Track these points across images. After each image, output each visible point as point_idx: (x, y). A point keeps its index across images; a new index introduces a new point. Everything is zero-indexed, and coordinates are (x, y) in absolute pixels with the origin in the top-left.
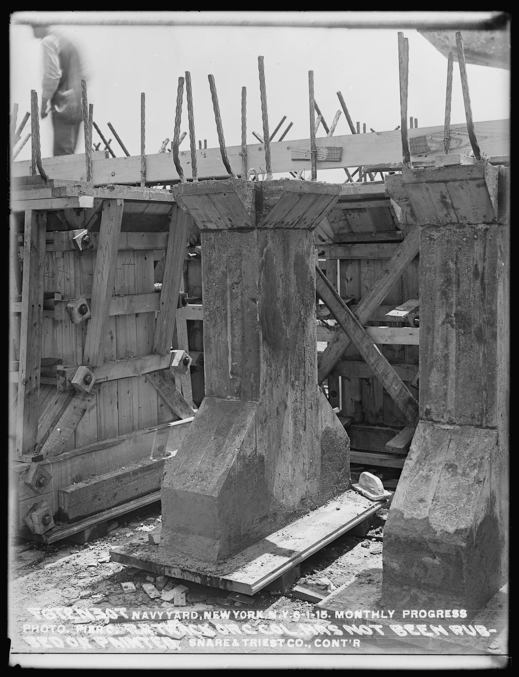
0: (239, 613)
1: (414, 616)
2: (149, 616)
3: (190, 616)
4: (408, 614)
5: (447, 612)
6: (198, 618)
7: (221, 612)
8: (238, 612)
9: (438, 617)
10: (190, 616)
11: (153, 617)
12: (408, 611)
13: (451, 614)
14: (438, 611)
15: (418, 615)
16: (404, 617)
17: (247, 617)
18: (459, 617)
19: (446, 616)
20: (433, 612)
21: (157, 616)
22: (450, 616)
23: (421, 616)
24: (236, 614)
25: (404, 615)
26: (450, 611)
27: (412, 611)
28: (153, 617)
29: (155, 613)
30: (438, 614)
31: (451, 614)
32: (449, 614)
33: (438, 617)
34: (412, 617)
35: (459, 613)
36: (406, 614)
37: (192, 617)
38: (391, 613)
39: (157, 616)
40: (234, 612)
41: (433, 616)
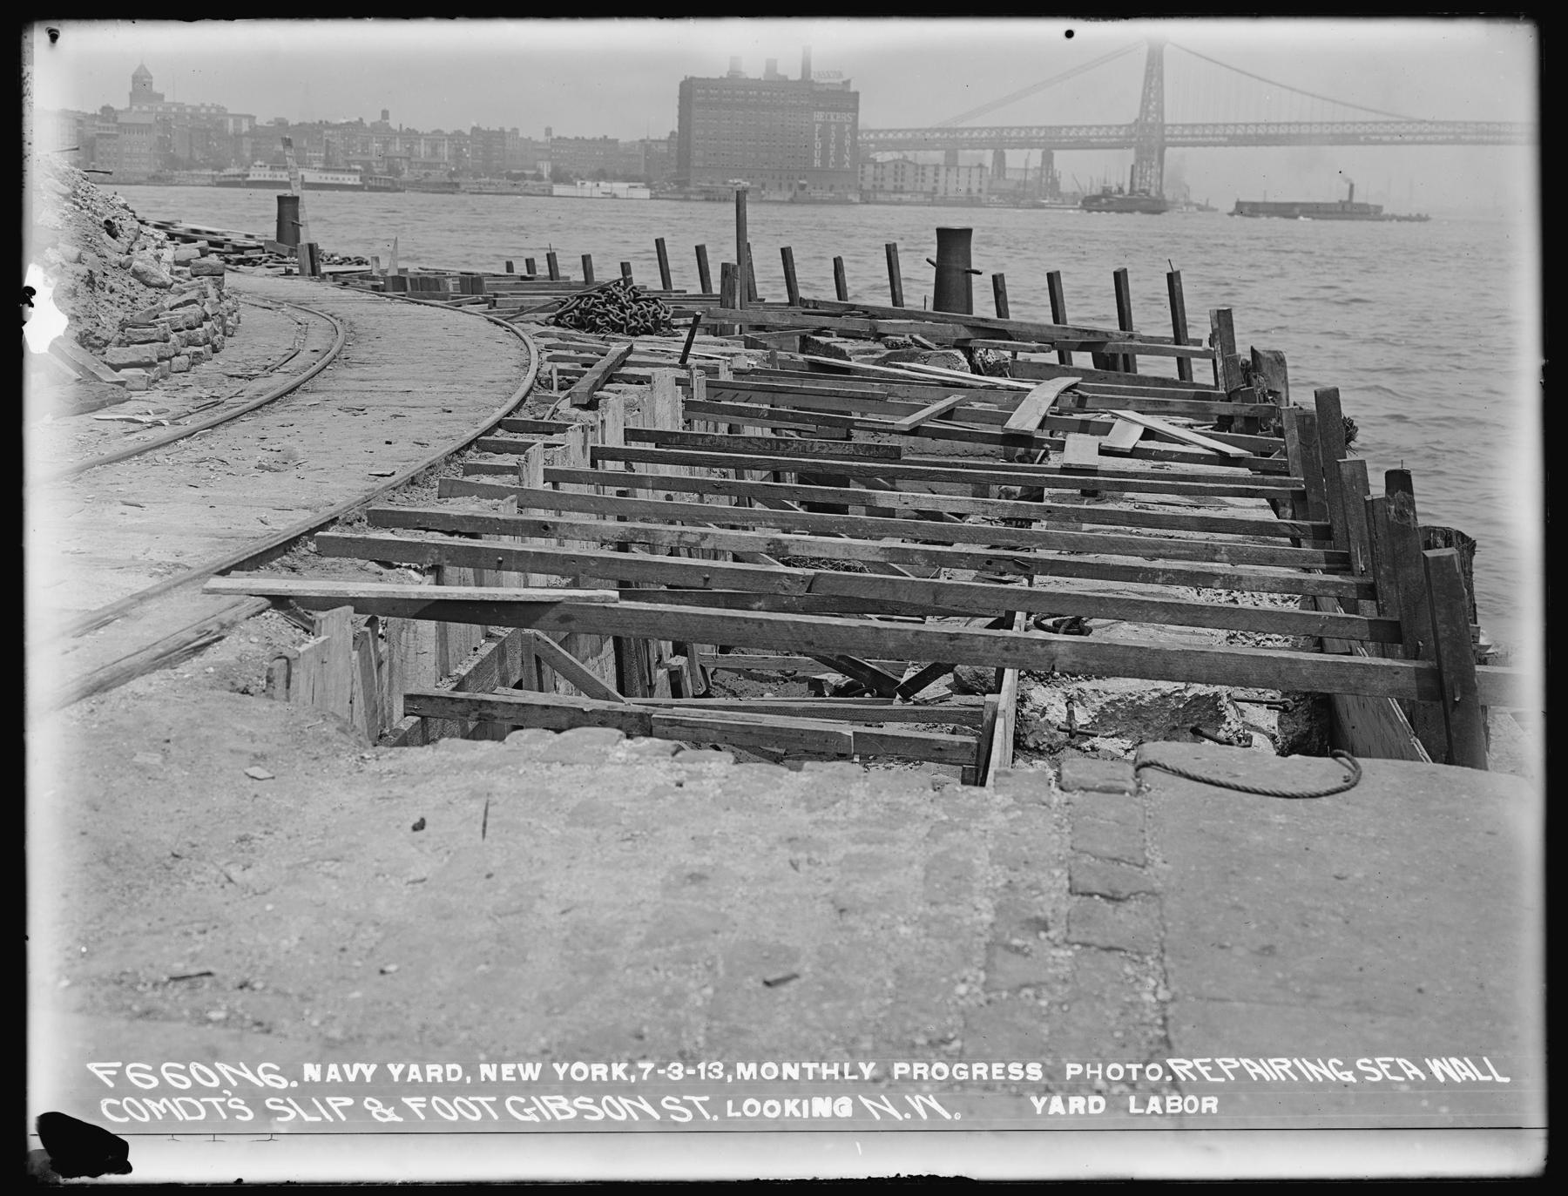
4: (906, 1071)
5: (997, 1068)
6: (463, 1079)
7: (520, 1066)
8: (566, 1065)
9: (975, 1077)
10: (444, 1076)
11: (352, 1078)
12: (907, 1066)
13: (1006, 1072)
14: (975, 1066)
16: (896, 1077)
18: (1024, 1080)
20: (964, 1066)
22: (1003, 1078)
24: (560, 1070)
25: (896, 1073)
26: (1002, 1065)
27: (916, 1065)
28: (352, 1078)
29: (357, 1066)
30: (975, 1073)
31: (1006, 1072)
32: (1001, 1072)
33: (975, 1077)
35: (1024, 1068)
36: (902, 1072)
37: (450, 1079)
38: (868, 1070)
40: (556, 1066)
41: (965, 1075)
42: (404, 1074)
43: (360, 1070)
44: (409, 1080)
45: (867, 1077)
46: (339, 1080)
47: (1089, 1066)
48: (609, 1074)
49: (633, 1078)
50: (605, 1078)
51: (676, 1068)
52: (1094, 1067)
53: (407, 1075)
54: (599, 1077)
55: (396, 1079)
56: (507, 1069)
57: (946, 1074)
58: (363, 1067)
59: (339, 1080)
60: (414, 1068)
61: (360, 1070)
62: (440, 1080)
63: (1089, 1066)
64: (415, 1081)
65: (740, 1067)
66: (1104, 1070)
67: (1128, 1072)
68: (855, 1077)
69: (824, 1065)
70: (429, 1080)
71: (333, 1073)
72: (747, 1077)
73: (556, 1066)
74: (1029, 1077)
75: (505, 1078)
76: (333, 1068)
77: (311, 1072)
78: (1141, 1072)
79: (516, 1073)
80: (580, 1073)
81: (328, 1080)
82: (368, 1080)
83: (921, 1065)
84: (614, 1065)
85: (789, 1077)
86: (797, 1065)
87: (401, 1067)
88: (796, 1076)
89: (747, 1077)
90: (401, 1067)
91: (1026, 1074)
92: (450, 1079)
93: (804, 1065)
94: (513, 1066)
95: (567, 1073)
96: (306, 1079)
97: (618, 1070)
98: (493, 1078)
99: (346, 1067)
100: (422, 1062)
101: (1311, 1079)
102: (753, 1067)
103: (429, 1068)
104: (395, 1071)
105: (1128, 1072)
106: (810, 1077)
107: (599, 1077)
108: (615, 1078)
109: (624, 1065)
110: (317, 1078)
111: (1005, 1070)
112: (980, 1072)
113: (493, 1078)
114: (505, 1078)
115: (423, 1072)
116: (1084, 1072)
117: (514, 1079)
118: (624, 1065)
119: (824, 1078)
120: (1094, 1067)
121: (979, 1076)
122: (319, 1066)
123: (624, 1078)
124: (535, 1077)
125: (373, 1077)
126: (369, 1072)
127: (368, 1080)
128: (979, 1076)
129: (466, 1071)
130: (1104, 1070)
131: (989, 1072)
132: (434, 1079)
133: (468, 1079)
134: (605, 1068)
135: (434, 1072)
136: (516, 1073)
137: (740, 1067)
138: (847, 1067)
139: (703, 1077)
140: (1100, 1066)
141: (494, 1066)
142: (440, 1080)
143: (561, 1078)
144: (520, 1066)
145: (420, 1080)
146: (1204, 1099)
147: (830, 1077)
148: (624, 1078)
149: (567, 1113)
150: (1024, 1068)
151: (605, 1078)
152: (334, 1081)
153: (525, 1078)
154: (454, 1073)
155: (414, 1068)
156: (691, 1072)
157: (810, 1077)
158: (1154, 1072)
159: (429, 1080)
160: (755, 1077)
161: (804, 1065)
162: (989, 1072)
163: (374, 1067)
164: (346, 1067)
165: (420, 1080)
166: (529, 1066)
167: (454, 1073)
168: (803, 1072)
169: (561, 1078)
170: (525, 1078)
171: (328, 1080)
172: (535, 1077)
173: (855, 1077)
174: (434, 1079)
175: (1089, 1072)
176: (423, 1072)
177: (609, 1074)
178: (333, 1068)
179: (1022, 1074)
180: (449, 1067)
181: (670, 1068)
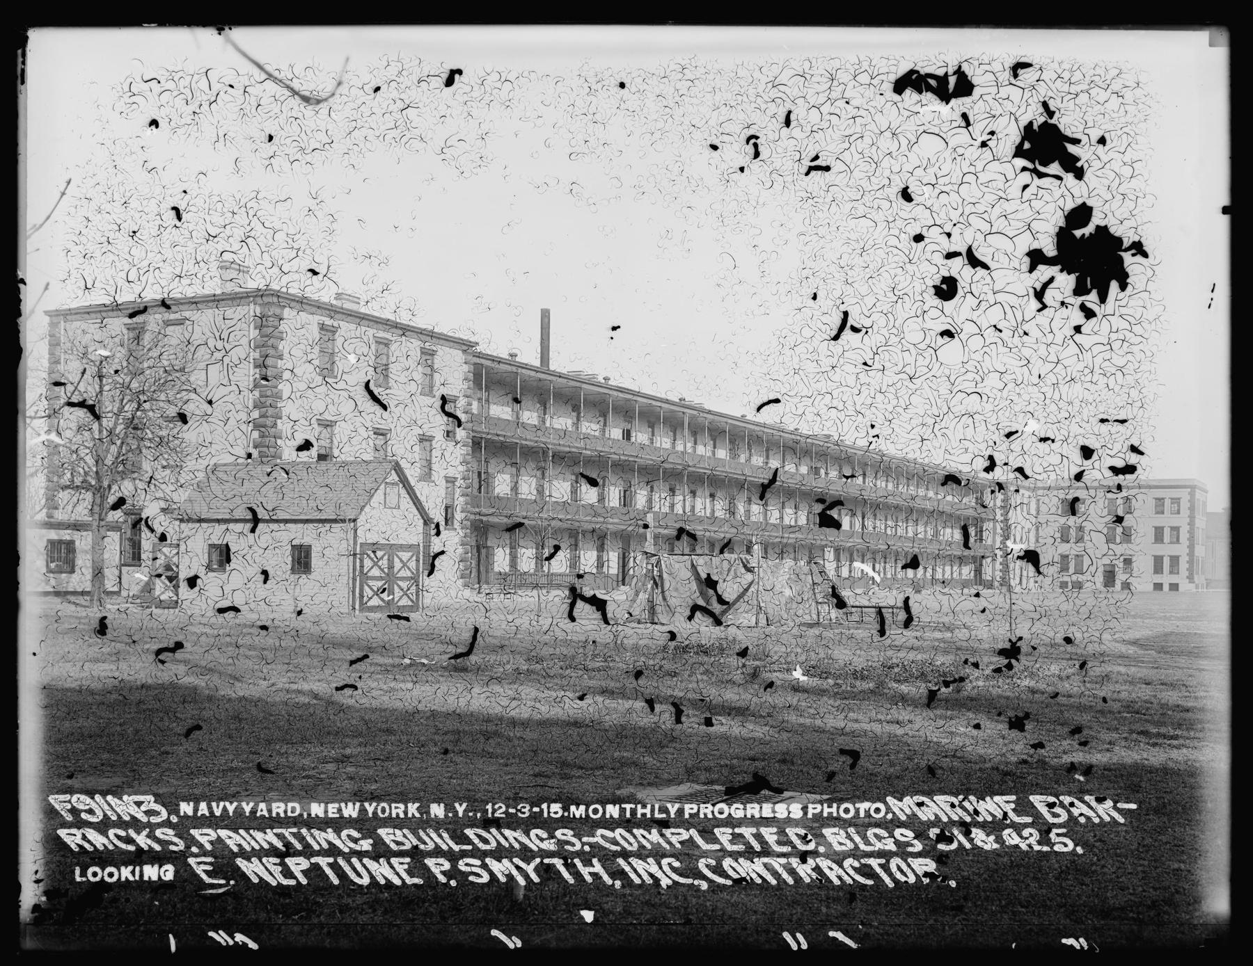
0: (376, 809)
1: (705, 815)
2: (210, 808)
3: (286, 812)
8: (374, 804)
9: (749, 816)
10: (286, 812)
11: (218, 813)
12: (695, 807)
14: (749, 806)
15: (713, 812)
17: (390, 813)
18: (788, 817)
20: (741, 806)
22: (772, 815)
23: (718, 815)
24: (370, 808)
28: (218, 813)
29: (222, 804)
37: (289, 814)
39: (225, 809)
40: (366, 805)
41: (739, 814)
42: (253, 812)
43: (225, 806)
46: (208, 815)
48: (406, 813)
50: (402, 816)
51: (524, 807)
53: (256, 812)
54: (398, 814)
58: (227, 804)
59: (208, 815)
61: (225, 809)
62: (282, 815)
63: (825, 805)
64: (263, 817)
65: (573, 808)
66: (838, 808)
69: (639, 806)
70: (274, 815)
71: (203, 808)
72: (578, 816)
73: (366, 805)
74: (791, 816)
76: (203, 806)
77: (186, 808)
80: (383, 811)
81: (199, 814)
83: (752, 805)
84: (410, 805)
85: (611, 816)
86: (617, 806)
90: (252, 804)
92: (289, 814)
93: (623, 806)
94: (336, 805)
95: (375, 813)
97: (413, 809)
98: (321, 815)
99: (214, 804)
100: (268, 802)
102: (582, 808)
103: (274, 805)
106: (628, 815)
107: (398, 814)
108: (410, 815)
109: (417, 805)
110: (190, 813)
112: (706, 811)
114: (331, 815)
117: (338, 816)
118: (417, 805)
119: (639, 816)
122: (192, 804)
123: (418, 815)
124: (355, 815)
126: (231, 808)
129: (302, 808)
132: (278, 814)
134: (402, 806)
135: (279, 808)
136: (340, 810)
137: (573, 808)
140: (835, 805)
141: (323, 805)
144: (343, 805)
147: (644, 815)
149: (403, 844)
150: (788, 809)
151: (402, 816)
153: (346, 815)
156: (536, 809)
157: (628, 815)
159: (274, 815)
161: (623, 806)
163: (235, 804)
166: (350, 805)
168: (623, 811)
169: (370, 815)
170: (346, 814)
171: (199, 814)
172: (355, 815)
174: (278, 814)
177: (406, 813)
178: (203, 806)
179: (785, 815)
180: (290, 805)
181: (519, 807)
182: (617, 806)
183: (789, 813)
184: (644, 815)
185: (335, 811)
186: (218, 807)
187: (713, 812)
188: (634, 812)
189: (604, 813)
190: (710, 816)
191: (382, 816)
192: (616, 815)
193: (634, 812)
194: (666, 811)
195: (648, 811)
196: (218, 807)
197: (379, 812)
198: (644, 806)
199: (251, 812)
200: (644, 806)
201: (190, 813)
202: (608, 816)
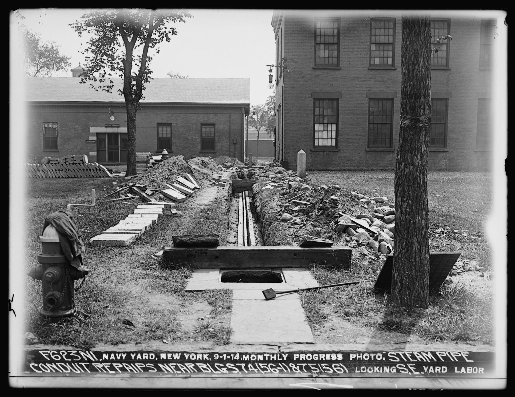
0: (189, 356)
1: (303, 359)
6: (155, 358)
8: (188, 355)
9: (320, 359)
10: (149, 357)
11: (119, 358)
12: (298, 355)
13: (331, 357)
15: (306, 357)
16: (295, 359)
18: (337, 360)
19: (327, 359)
20: (317, 355)
21: (121, 357)
22: (330, 359)
26: (330, 355)
27: (301, 355)
28: (119, 358)
30: (321, 357)
31: (331, 357)
33: (320, 359)
34: (301, 359)
39: (121, 356)
41: (317, 358)
44: (137, 359)
45: (285, 359)
46: (114, 359)
47: (357, 354)
49: (210, 359)
52: (359, 355)
53: (136, 357)
55: (133, 359)
56: (169, 356)
57: (311, 358)
58: (123, 354)
59: (114, 359)
60: (139, 355)
61: (121, 356)
62: (147, 358)
64: (139, 359)
67: (370, 357)
68: (281, 359)
69: (271, 355)
70: (144, 358)
72: (246, 360)
74: (338, 359)
75: (168, 358)
78: (375, 357)
79: (172, 357)
80: (193, 357)
81: (111, 359)
82: (124, 359)
87: (135, 354)
88: (262, 359)
89: (246, 360)
90: (135, 354)
91: (337, 358)
92: (150, 358)
93: (265, 355)
95: (189, 358)
96: (104, 359)
98: (165, 358)
99: (117, 355)
101: (453, 360)
104: (133, 356)
105: (370, 357)
106: (267, 359)
108: (204, 359)
110: (107, 358)
111: (330, 356)
113: (165, 358)
114: (168, 358)
115: (142, 356)
116: (356, 357)
117: (171, 359)
119: (271, 359)
120: (359, 355)
121: (322, 359)
122: (108, 354)
123: (208, 359)
125: (125, 358)
126: (124, 356)
127: (124, 359)
128: (322, 359)
130: (363, 356)
131: (325, 358)
133: (157, 359)
138: (279, 355)
139: (233, 359)
142: (147, 358)
143: (187, 359)
144: (174, 354)
145: (141, 359)
146: (479, 368)
147: (273, 359)
148: (208, 359)
150: (336, 356)
152: (113, 359)
153: (175, 358)
154: (152, 357)
155: (139, 355)
157: (267, 359)
158: (379, 357)
159: (144, 358)
160: (248, 360)
161: (265, 355)
162: (325, 358)
164: (117, 355)
165: (141, 359)
167: (152, 357)
169: (187, 359)
170: (175, 358)
171: (111, 359)
172: (178, 358)
173: (281, 359)
175: (358, 357)
176: (142, 356)
179: (335, 358)
182: (262, 355)
183: (337, 358)
184: (273, 359)
185: (171, 357)
186: (118, 356)
187: (306, 357)
188: (269, 357)
189: (257, 358)
190: (304, 359)
191: (192, 359)
192: (262, 359)
193: (269, 357)
194: (283, 357)
195: (275, 358)
196: (118, 356)
197: (191, 357)
198: (273, 356)
199: (134, 358)
200: (273, 356)
201: (107, 358)
202: (258, 360)
